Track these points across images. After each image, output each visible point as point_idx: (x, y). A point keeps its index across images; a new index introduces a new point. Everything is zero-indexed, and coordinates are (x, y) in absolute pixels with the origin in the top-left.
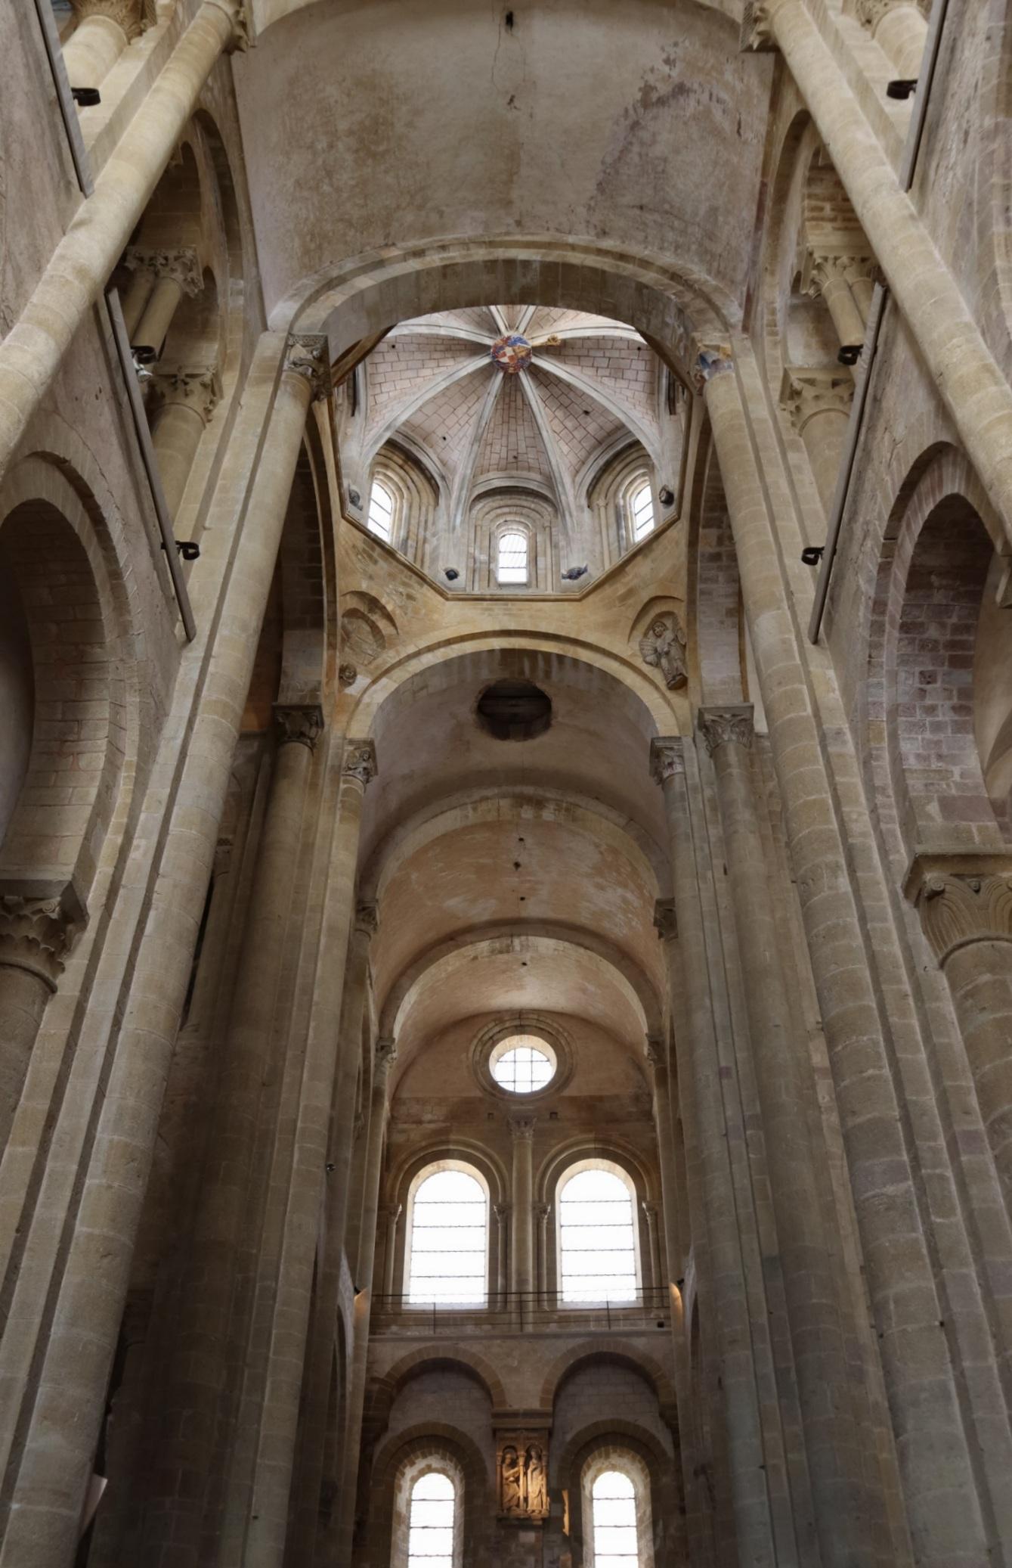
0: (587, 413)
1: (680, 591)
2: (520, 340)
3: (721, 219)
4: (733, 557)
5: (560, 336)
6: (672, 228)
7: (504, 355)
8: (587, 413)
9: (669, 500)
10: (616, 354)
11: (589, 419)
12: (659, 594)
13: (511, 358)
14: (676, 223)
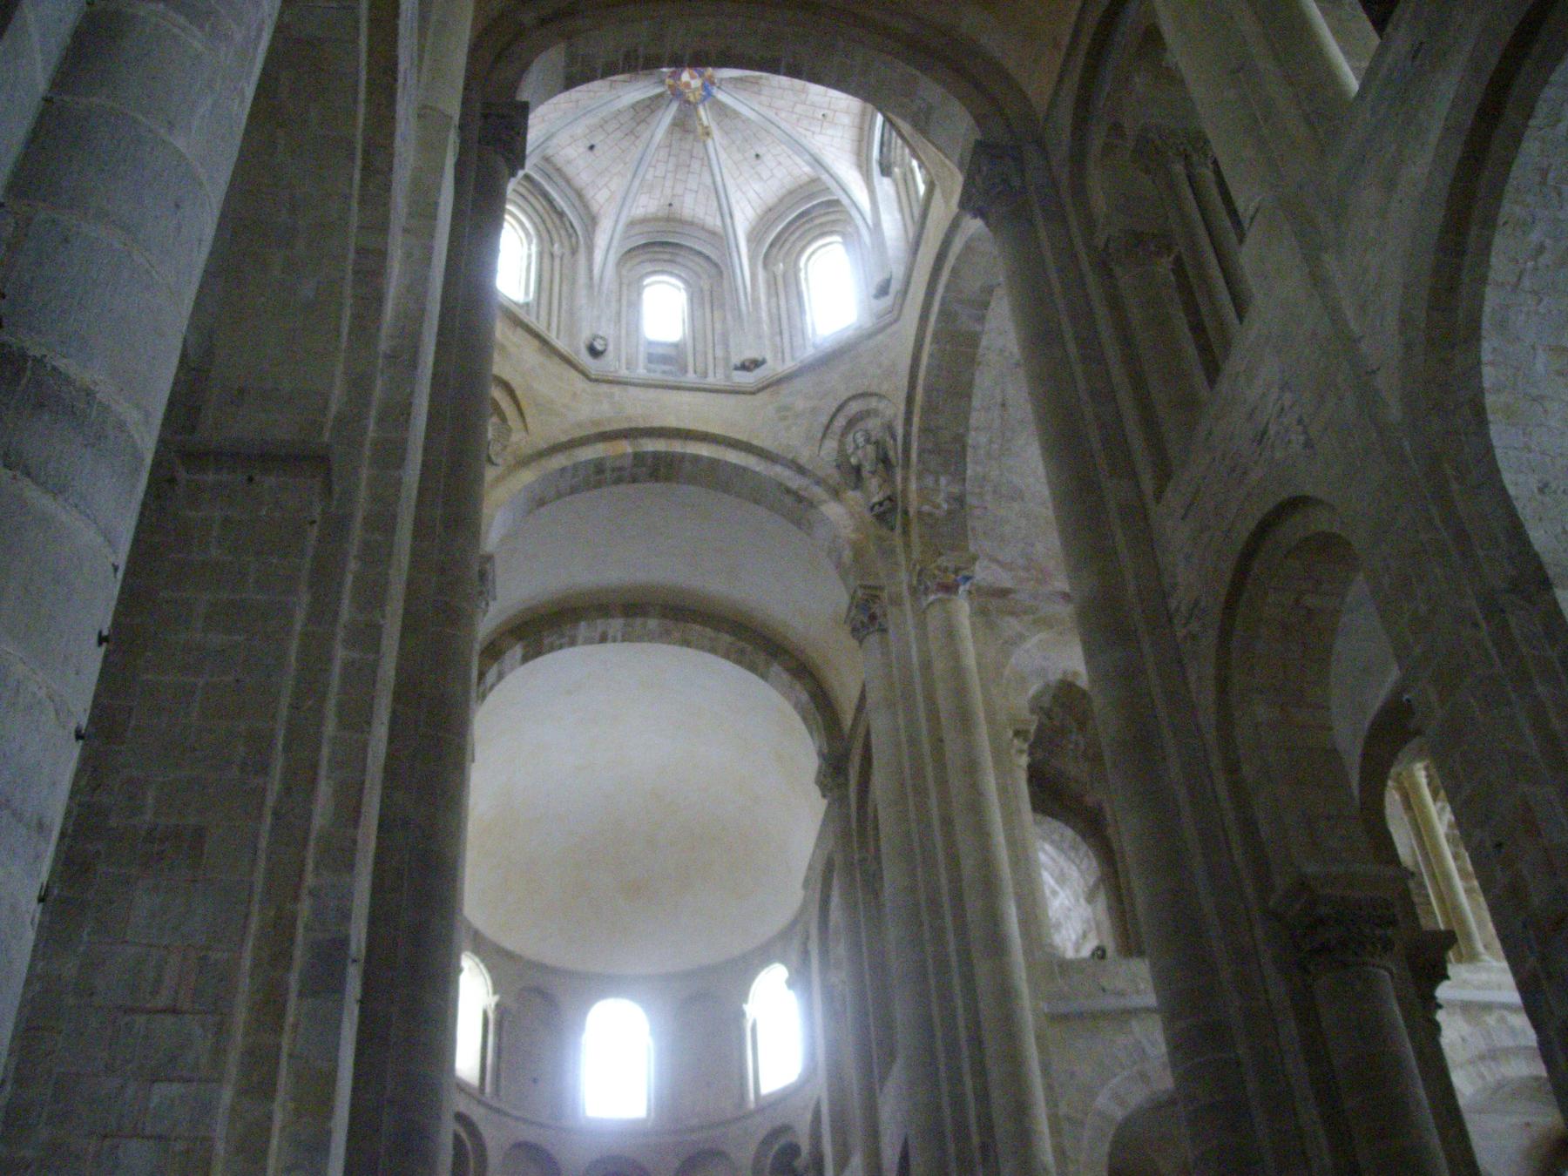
0: (592, 147)
1: (542, 430)
2: (709, 94)
3: (1016, 506)
4: (599, 484)
5: (710, 142)
6: (991, 442)
7: (692, 77)
8: (592, 147)
9: (594, 352)
10: (668, 183)
11: (581, 150)
12: (519, 393)
13: (688, 85)
14: (995, 446)
